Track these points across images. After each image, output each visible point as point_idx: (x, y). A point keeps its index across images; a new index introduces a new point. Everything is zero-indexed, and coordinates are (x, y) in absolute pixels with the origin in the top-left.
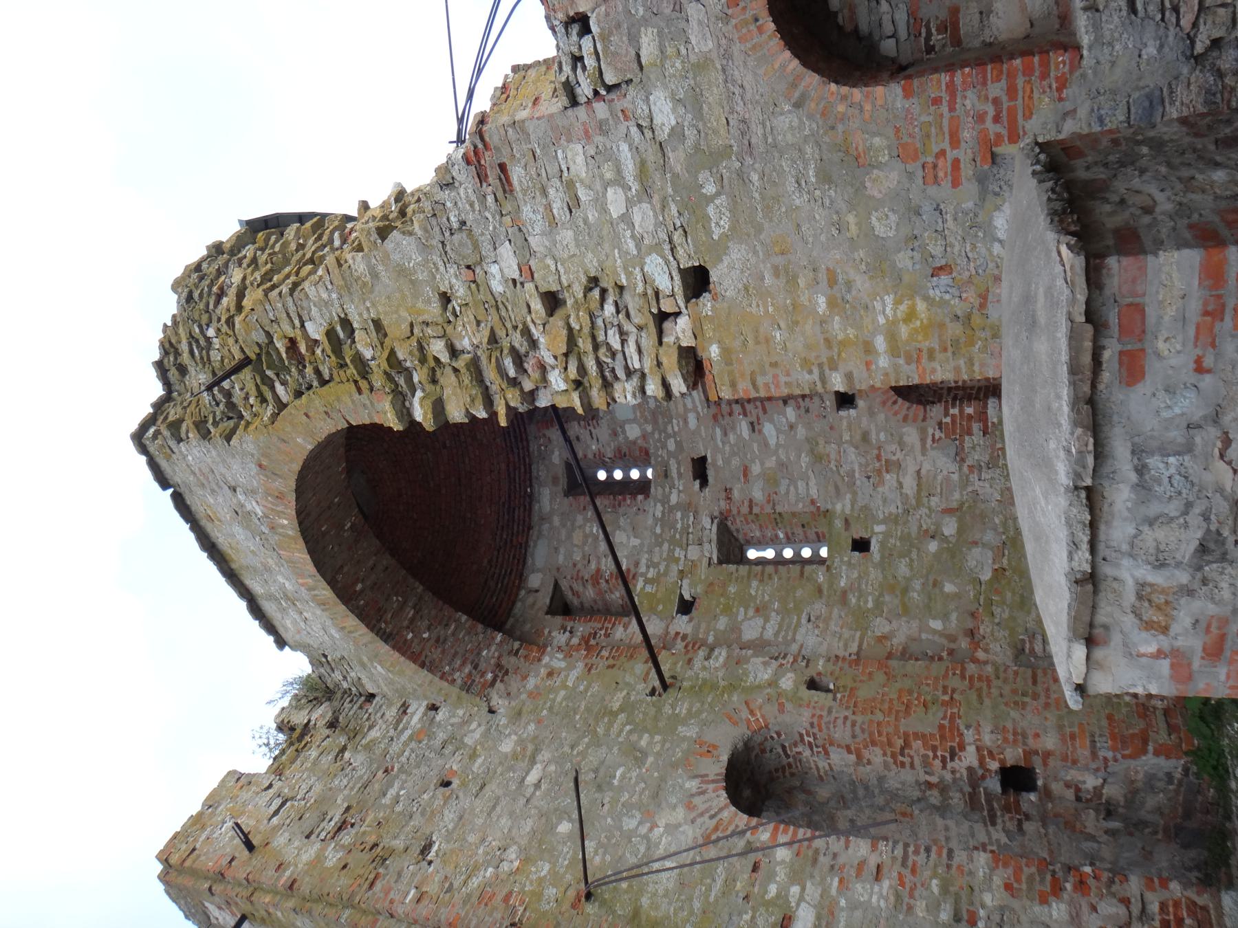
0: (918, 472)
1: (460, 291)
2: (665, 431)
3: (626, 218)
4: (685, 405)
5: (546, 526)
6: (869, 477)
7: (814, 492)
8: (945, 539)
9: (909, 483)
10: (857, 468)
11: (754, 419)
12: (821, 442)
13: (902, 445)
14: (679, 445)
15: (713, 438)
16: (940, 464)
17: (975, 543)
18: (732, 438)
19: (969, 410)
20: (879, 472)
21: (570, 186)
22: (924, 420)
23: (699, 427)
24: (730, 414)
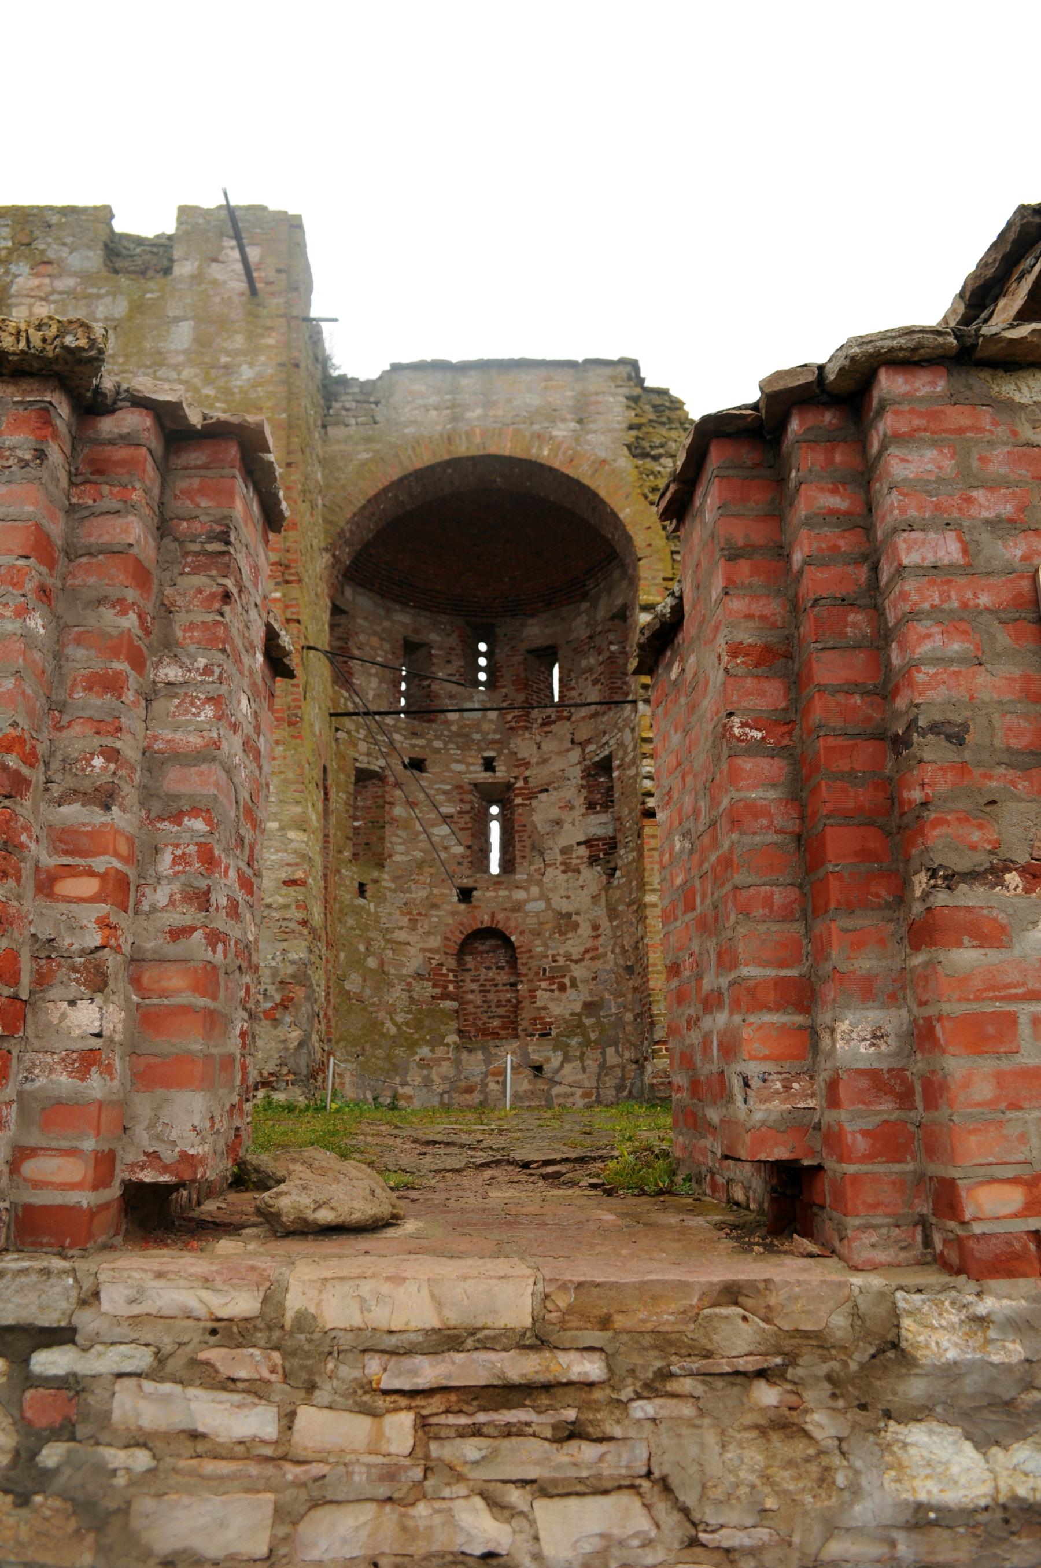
0: (408, 944)
2: (450, 741)
4: (473, 764)
5: (382, 612)
6: (405, 904)
7: (397, 858)
8: (365, 959)
9: (401, 936)
10: (413, 896)
11: (455, 819)
12: (432, 870)
13: (428, 934)
14: (437, 751)
15: (442, 782)
16: (414, 962)
17: (364, 981)
18: (441, 798)
19: (451, 987)
20: (409, 913)
22: (446, 953)
23: (452, 771)
24: (461, 800)
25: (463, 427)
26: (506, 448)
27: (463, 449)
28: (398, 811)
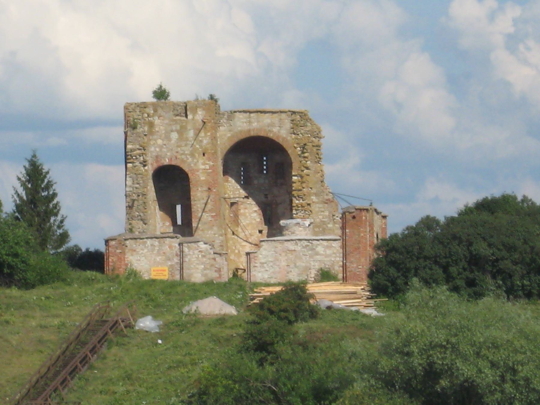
1: (312, 191)
3: (318, 218)
21: (323, 212)
25: (252, 128)
26: (262, 134)
27: (252, 134)
28: (242, 211)
